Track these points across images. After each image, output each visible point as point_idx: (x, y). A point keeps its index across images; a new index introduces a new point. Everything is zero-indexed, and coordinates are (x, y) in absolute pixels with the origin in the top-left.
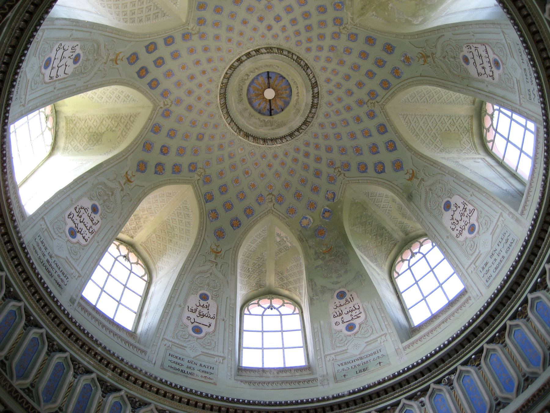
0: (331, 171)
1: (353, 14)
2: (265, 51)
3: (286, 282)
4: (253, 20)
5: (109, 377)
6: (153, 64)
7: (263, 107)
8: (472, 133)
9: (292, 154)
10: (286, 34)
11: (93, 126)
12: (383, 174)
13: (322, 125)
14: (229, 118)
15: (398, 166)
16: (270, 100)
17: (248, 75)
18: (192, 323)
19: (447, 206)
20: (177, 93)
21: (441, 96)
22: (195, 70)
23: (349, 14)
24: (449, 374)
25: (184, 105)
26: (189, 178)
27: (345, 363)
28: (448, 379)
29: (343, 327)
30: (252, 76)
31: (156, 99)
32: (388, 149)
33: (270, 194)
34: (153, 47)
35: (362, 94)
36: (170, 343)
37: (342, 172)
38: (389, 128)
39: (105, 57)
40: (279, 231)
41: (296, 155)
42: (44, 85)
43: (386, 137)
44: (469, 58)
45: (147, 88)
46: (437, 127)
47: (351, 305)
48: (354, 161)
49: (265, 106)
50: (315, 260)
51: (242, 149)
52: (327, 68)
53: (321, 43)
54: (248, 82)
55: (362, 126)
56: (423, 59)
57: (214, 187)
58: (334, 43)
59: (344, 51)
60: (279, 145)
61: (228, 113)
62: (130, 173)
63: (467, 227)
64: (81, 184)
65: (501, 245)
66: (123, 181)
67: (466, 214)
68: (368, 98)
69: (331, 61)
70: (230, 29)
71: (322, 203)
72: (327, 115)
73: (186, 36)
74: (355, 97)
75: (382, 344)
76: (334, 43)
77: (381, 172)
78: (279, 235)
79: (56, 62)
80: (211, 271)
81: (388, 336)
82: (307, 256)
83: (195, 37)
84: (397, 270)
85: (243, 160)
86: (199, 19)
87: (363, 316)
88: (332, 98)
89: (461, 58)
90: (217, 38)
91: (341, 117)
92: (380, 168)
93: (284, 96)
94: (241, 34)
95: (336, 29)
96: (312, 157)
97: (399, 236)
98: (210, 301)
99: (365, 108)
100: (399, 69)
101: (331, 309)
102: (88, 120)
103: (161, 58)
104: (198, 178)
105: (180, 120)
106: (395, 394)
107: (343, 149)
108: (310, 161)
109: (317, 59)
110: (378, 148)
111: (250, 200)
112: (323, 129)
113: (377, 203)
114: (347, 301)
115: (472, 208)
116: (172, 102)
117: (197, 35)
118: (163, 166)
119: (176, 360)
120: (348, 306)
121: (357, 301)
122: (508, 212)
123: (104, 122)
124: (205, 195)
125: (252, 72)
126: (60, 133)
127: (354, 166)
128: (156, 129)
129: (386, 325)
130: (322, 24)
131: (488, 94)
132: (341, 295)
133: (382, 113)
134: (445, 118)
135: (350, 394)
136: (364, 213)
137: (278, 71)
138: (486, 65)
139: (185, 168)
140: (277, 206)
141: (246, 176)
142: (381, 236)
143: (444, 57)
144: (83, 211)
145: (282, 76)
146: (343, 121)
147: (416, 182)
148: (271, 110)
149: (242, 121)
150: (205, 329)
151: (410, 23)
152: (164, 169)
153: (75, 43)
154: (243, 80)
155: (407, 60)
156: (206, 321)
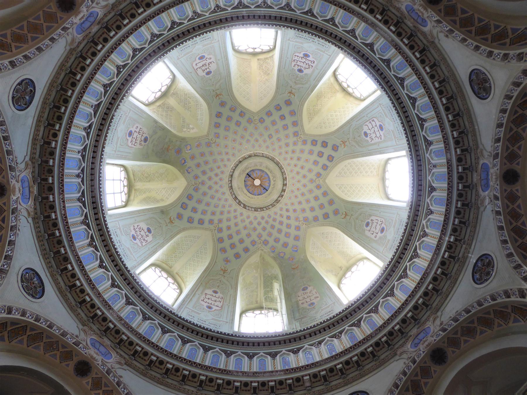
0: (200, 180)
1: (265, 252)
2: (279, 199)
4: (298, 207)
5: (243, 11)
7: (254, 174)
9: (223, 169)
10: (278, 215)
13: (224, 194)
15: (180, 217)
19: (149, 231)
20: (300, 146)
21: (194, 261)
22: (300, 163)
23: (266, 251)
27: (120, 119)
28: (81, 176)
29: (133, 130)
32: (190, 217)
35: (224, 225)
38: (200, 226)
39: (351, 142)
40: (195, 130)
41: (220, 170)
44: (216, 294)
45: (316, 139)
47: (138, 142)
49: (254, 175)
51: (246, 148)
53: (261, 226)
54: (271, 178)
55: (209, 213)
57: (244, 121)
59: (250, 234)
60: (232, 166)
61: (268, 158)
63: (136, 235)
64: (317, 78)
65: (123, 251)
66: (293, 91)
67: (142, 239)
71: (190, 163)
72: (226, 200)
73: (319, 175)
74: (224, 220)
77: (182, 205)
78: (193, 128)
81: (113, 152)
82: (175, 136)
83: (314, 178)
85: (241, 144)
86: (321, 187)
87: (130, 144)
89: (217, 290)
91: (220, 206)
92: (184, 206)
93: (250, 188)
94: (296, 197)
95: (263, 239)
96: (213, 176)
97: (139, 185)
98: (204, 74)
99: (216, 221)
100: (225, 253)
101: (145, 130)
103: (321, 157)
106: (94, 140)
107: (205, 195)
108: (212, 174)
109: (256, 218)
111: (221, 131)
113: (166, 189)
114: (142, 141)
115: (144, 244)
117: (314, 179)
119: (205, 38)
120: (139, 139)
121: (138, 146)
122: (136, 265)
123: (320, 106)
124: (245, 114)
125: (274, 184)
126: (336, 82)
128: (295, 124)
130: (270, 235)
131: (195, 291)
132: (146, 140)
135: (113, 115)
137: (264, 195)
138: (210, 301)
139: (265, 117)
140: (207, 141)
142: (146, 177)
143: (220, 281)
144: (307, 67)
145: (260, 195)
146: (218, 206)
148: (250, 176)
149: (258, 160)
150: (198, 61)
151: (243, 274)
153: (373, 142)
154: (274, 177)
155: (227, 261)
156: (200, 65)
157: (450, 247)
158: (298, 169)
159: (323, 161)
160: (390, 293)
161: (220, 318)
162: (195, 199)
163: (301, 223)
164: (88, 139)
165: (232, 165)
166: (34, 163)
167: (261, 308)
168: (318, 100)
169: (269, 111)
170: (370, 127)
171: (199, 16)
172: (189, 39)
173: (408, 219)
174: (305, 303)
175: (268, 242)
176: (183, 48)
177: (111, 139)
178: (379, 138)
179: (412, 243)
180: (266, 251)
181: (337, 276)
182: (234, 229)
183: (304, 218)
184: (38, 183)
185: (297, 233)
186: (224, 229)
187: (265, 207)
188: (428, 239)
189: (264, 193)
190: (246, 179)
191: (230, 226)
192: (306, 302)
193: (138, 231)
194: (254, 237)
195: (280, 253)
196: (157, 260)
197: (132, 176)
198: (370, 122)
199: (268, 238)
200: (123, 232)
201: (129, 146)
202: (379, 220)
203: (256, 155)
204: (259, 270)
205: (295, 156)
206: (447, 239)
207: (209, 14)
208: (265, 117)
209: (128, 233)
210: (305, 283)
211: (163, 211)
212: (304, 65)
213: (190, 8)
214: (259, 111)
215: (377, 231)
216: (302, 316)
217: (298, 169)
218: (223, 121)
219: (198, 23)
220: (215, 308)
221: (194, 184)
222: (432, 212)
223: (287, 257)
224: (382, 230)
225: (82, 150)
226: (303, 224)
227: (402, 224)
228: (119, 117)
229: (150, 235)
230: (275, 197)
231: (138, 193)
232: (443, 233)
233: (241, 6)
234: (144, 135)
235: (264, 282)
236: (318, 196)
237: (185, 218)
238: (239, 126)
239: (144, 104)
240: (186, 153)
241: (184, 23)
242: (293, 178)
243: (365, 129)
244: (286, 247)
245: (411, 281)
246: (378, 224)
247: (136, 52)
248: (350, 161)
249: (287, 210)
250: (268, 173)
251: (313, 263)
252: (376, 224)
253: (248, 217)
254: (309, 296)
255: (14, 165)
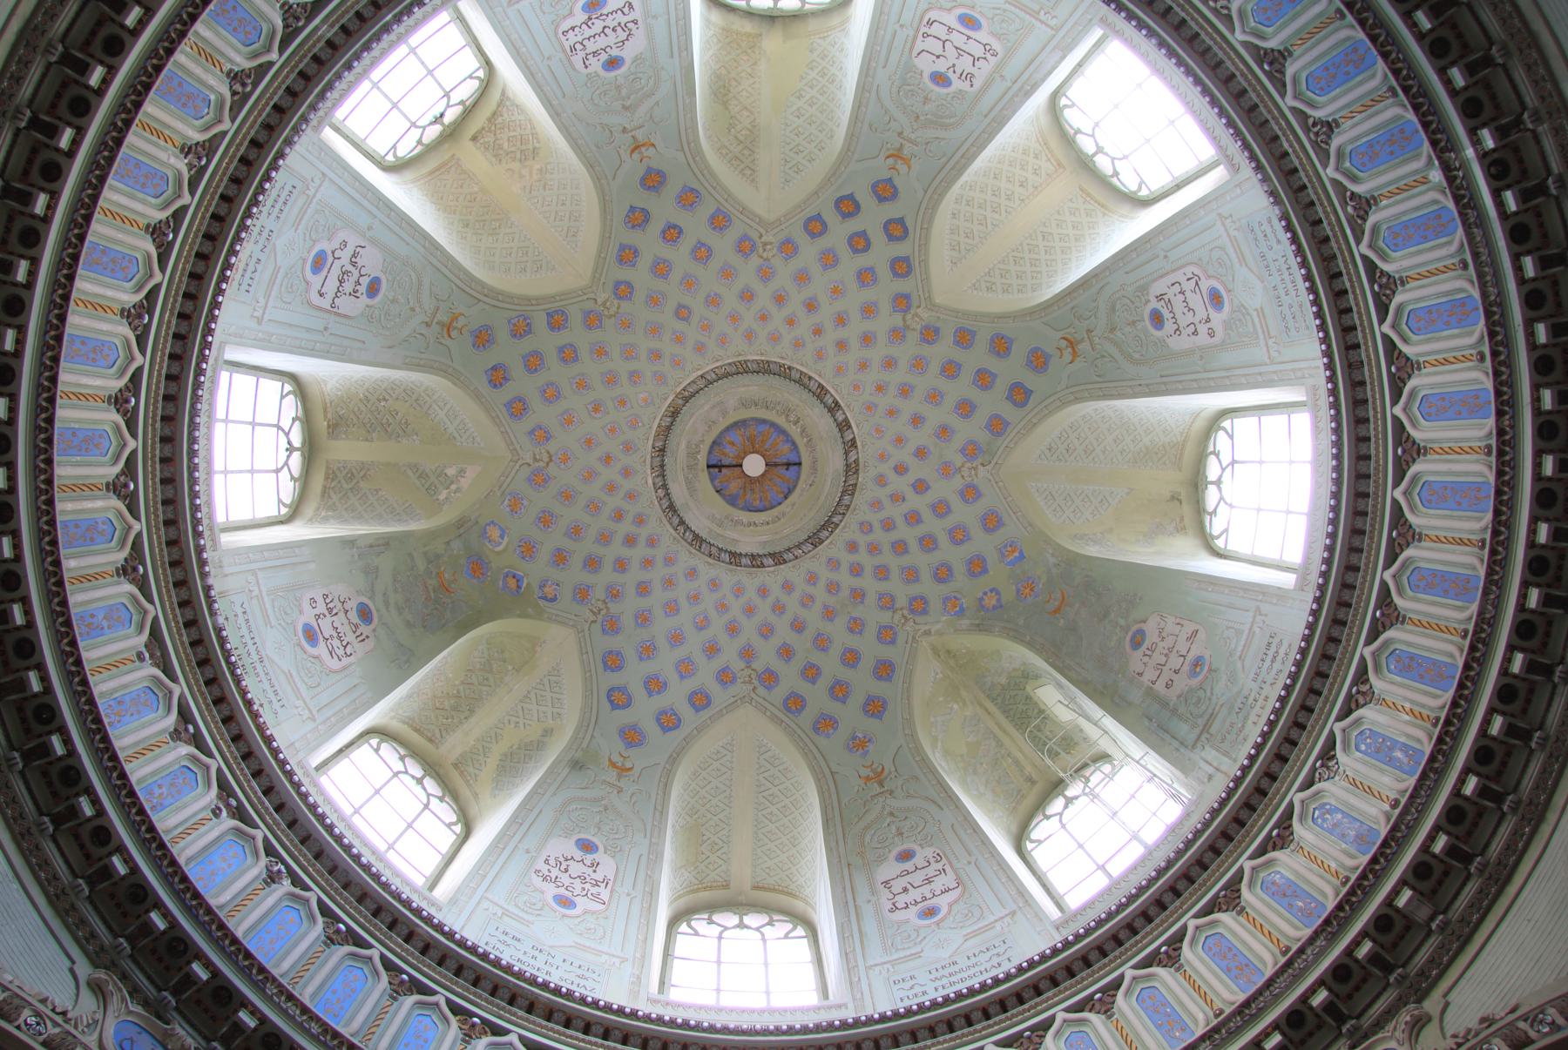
0: (599, 593)
1: (940, 633)
3: (345, 486)
4: (918, 438)
5: (317, 28)
6: (859, 228)
7: (727, 451)
8: (697, 890)
9: (632, 510)
10: (886, 502)
11: (740, 88)
12: (608, 705)
13: (692, 573)
14: (714, 376)
15: (632, 737)
16: (741, 466)
17: (796, 423)
18: (333, 252)
19: (587, 847)
20: (784, 273)
21: (774, 819)
23: (938, 626)
24: (291, 873)
25: (757, 285)
26: (603, 280)
28: (279, 871)
29: (308, 616)
30: (794, 431)
31: (783, 227)
33: (550, 457)
34: (897, 233)
36: (311, 193)
37: (600, 617)
38: (705, 714)
39: (913, 136)
40: (472, 472)
41: (629, 518)
42: (926, 6)
43: (685, 711)
44: (914, 861)
45: (810, 211)
46: (709, 816)
47: (350, 637)
48: (623, 642)
50: (425, 554)
51: (645, 400)
52: (814, 584)
54: (781, 421)
55: (699, 658)
56: (871, 774)
58: (871, 598)
59: (855, 619)
61: (727, 375)
62: (652, 149)
63: (562, 891)
65: (567, 966)
67: (587, 886)
68: (760, 669)
69: (830, 592)
70: (905, 391)
71: (536, 571)
73: (902, 302)
74: (757, 642)
75: (295, 711)
76: (871, 598)
77: (611, 702)
78: (462, 472)
79: (958, 39)
80: (418, 310)
81: (310, 725)
82: (432, 535)
83: (897, 320)
84: (384, 745)
85: (622, 402)
86: (937, 331)
87: (334, 664)
88: (751, 593)
90: (890, 363)
91: (713, 613)
92: (618, 699)
93: (748, 497)
94: (892, 413)
95: (902, 601)
96: (625, 552)
98: (364, 300)
99: (737, 665)
100: (836, 729)
101: (339, 590)
102: (752, 81)
104: (600, 301)
105: (727, 273)
106: (226, 742)
107: (646, 620)
108: (617, 549)
109: (834, 564)
110: (659, 692)
111: (543, 413)
112: (686, 576)
113: (532, 696)
114: (356, 626)
115: (605, 895)
116: (767, 259)
118: (640, 226)
119: (281, 200)
120: (345, 629)
121: (359, 649)
123: (746, 113)
126: (731, 17)
127: (614, 642)
128: (719, 221)
129: (329, 718)
130: (911, 575)
132: (365, 614)
133: (733, 700)
134: (725, 832)
135: (219, 630)
136: (510, 668)
137: (801, 484)
138: (914, 894)
139: (625, 274)
141: (590, 407)
142: (455, 708)
143: (892, 814)
145: (790, 491)
146: (706, 618)
147: (611, 776)
148: (720, 467)
150: (316, 281)
152: (633, 227)
153: (978, 83)
154: (786, 412)
156: (331, 286)
157: (1498, 170)
158: (832, 335)
159: (882, 252)
160: (1404, 451)
161: (982, 916)
162: (630, 654)
163: (965, 472)
164: (210, 755)
165: (645, 479)
166: (114, 964)
167: (1056, 787)
168: (725, 104)
169: (623, 247)
170: (936, 47)
171: (209, 147)
172: (238, 239)
173: (1277, 201)
174: (1175, 677)
175: (922, 598)
176: (247, 280)
177: (271, 695)
178: (988, 56)
179: (1344, 261)
180: (938, 626)
181: (1184, 528)
182: (802, 645)
183: (963, 451)
184: (177, 1009)
185: (980, 508)
186: (777, 665)
187: (834, 513)
188: (1386, 207)
189: (798, 478)
190: (716, 483)
191: (785, 644)
192: (1176, 672)
193: (561, 875)
194: (874, 617)
195: (981, 599)
196: (676, 899)
197: (415, 738)
198: (926, 35)
199: (915, 590)
200: (521, 914)
201: (336, 672)
202: (1182, 279)
203: (687, 397)
204: (964, 693)
205: (795, 305)
206: (1470, 152)
207: (233, 121)
208: (625, 274)
209: (539, 906)
210: (1122, 622)
211: (577, 765)
212: (612, 38)
213: (165, 150)
214: (595, 271)
215: (1201, 313)
216: (1201, 722)
217: (832, 335)
218: (523, 384)
219: (224, 174)
220: (943, 902)
221: (592, 618)
222: (1330, 127)
223: (1008, 594)
224: (1216, 299)
225: (219, 797)
226: (975, 469)
227: (1260, 236)
228: (241, 620)
229: (599, 856)
230: (834, 461)
231: (471, 769)
232: (1442, 146)
233: (298, 19)
234: (347, 606)
235: (1006, 712)
236: (951, 362)
237: (650, 727)
238: (576, 359)
239: (282, 523)
240: (498, 553)
241: (185, 208)
242: (839, 370)
243: (926, 65)
244: (985, 571)
245: (1441, 368)
246: (1188, 294)
247: (127, 401)
248: (956, 190)
249: (901, 470)
250: (761, 414)
251: (1093, 551)
252: (1181, 297)
253: (812, 579)
254: (1170, 650)
255: (57, 1030)
